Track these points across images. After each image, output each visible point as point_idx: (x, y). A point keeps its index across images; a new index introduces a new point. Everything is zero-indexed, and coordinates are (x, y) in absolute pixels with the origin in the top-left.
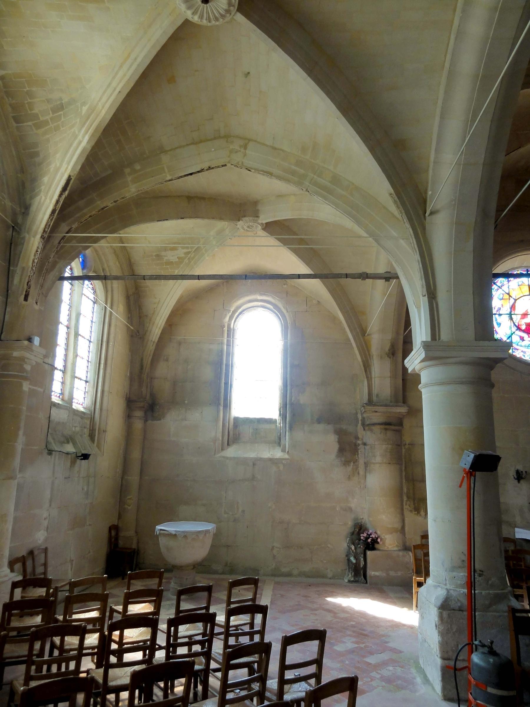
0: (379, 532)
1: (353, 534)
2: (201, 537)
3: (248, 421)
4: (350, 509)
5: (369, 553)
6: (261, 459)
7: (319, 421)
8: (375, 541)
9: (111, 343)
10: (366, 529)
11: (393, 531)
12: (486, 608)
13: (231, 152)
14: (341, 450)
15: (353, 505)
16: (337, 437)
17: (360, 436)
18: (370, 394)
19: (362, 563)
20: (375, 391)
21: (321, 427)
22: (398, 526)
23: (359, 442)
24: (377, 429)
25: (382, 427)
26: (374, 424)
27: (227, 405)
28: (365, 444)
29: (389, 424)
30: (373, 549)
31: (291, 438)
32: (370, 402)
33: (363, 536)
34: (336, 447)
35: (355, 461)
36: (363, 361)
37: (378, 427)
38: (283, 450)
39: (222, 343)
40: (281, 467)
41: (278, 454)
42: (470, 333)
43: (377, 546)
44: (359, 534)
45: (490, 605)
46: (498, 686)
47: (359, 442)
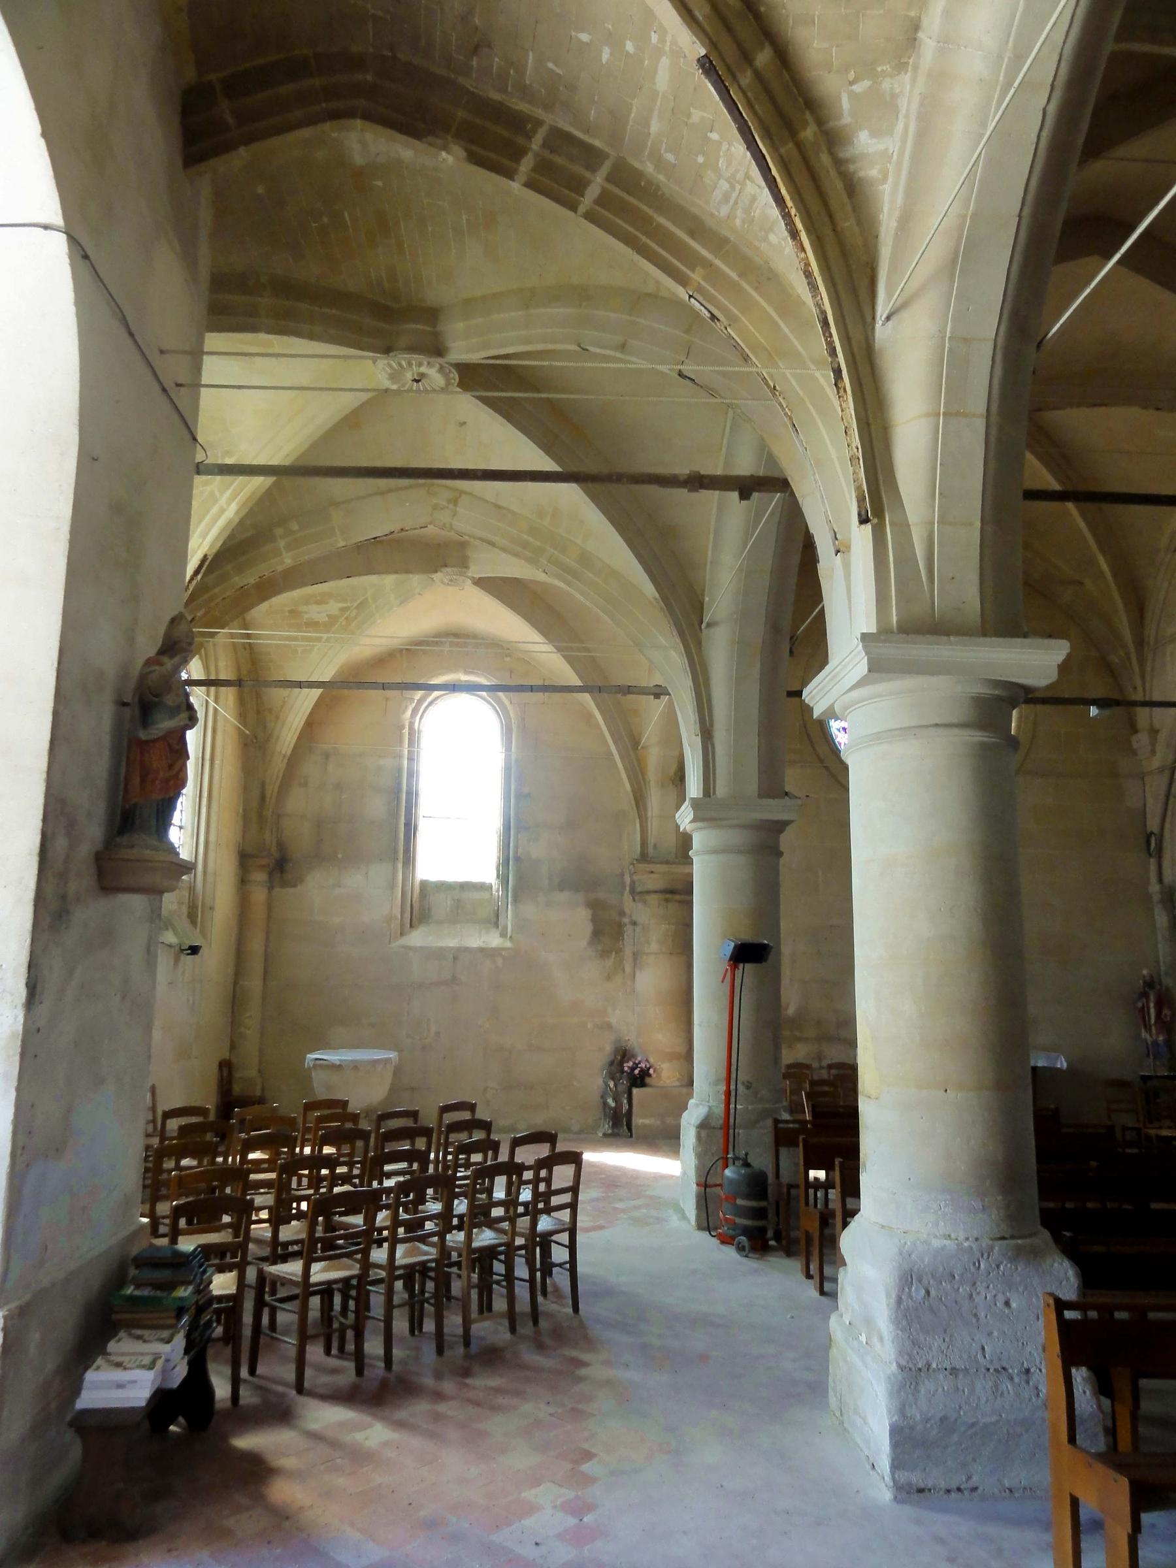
0: (651, 1060)
1: (612, 1063)
2: (380, 1068)
3: (443, 887)
4: (609, 1026)
5: (635, 1091)
6: (467, 950)
7: (561, 888)
8: (645, 1073)
9: (217, 762)
10: (633, 1056)
12: (752, 1124)
13: (435, 507)
15: (613, 1020)
16: (590, 912)
17: (627, 910)
18: (644, 844)
19: (625, 1107)
20: (651, 841)
21: (562, 897)
22: (682, 1049)
23: (626, 920)
24: (653, 899)
25: (661, 896)
26: (649, 892)
27: (409, 859)
28: (634, 923)
29: (672, 892)
30: (643, 1085)
31: (516, 915)
32: (644, 857)
33: (627, 1066)
34: (588, 929)
35: (619, 951)
36: (634, 791)
37: (655, 896)
38: (503, 935)
39: (400, 756)
40: (500, 962)
41: (494, 940)
42: (752, 787)
43: (648, 1080)
44: (621, 1064)
45: (757, 1122)
46: (748, 1197)
47: (626, 920)
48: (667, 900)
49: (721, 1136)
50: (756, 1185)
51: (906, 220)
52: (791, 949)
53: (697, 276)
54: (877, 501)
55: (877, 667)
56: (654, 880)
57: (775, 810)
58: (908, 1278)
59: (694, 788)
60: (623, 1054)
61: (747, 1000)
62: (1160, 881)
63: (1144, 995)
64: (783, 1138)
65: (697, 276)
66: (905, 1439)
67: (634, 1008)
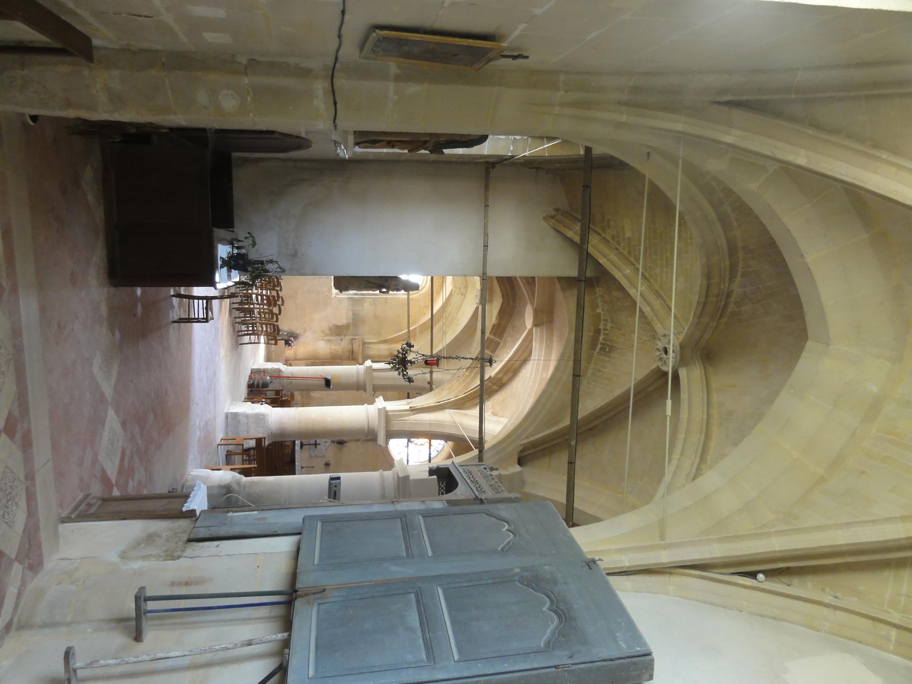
4: (305, 331)
7: (354, 314)
8: (290, 345)
11: (296, 354)
14: (337, 327)
20: (370, 346)
21: (351, 316)
32: (364, 343)
34: (340, 324)
35: (332, 335)
42: (376, 383)
49: (277, 375)
50: (265, 385)
51: (466, 415)
52: (325, 393)
53: (467, 373)
54: (415, 410)
55: (379, 410)
56: (357, 346)
57: (369, 389)
58: (264, 415)
59: (376, 366)
60: (296, 337)
61: (315, 382)
64: (278, 392)
65: (467, 373)
66: (236, 415)
67: (313, 341)
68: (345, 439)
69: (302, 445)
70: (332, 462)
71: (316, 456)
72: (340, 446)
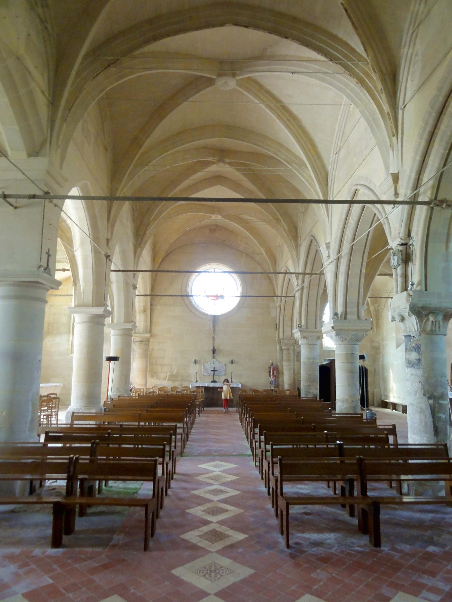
22: (144, 383)
24: (137, 343)
48: (141, 344)
62: (279, 337)
63: (270, 368)
68: (212, 348)
69: (214, 381)
70: (230, 359)
71: (225, 370)
72: (216, 351)
